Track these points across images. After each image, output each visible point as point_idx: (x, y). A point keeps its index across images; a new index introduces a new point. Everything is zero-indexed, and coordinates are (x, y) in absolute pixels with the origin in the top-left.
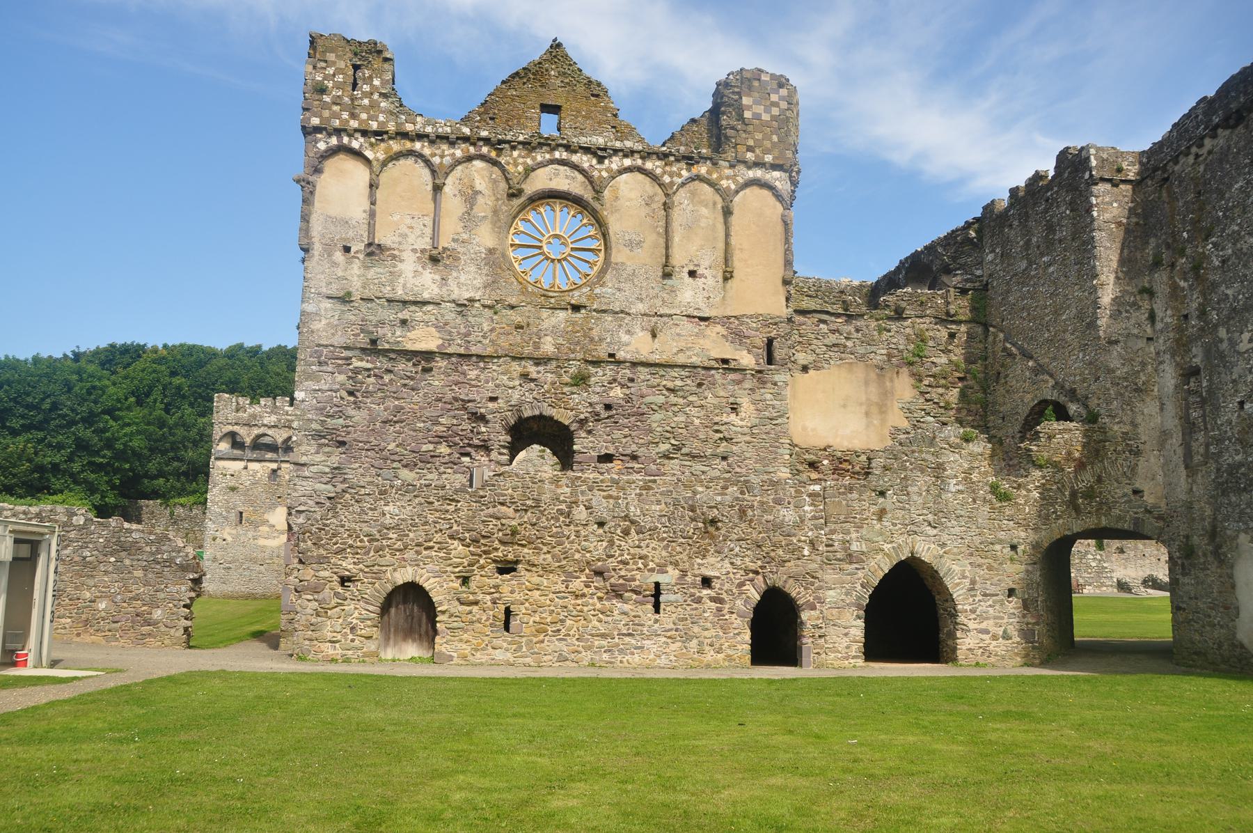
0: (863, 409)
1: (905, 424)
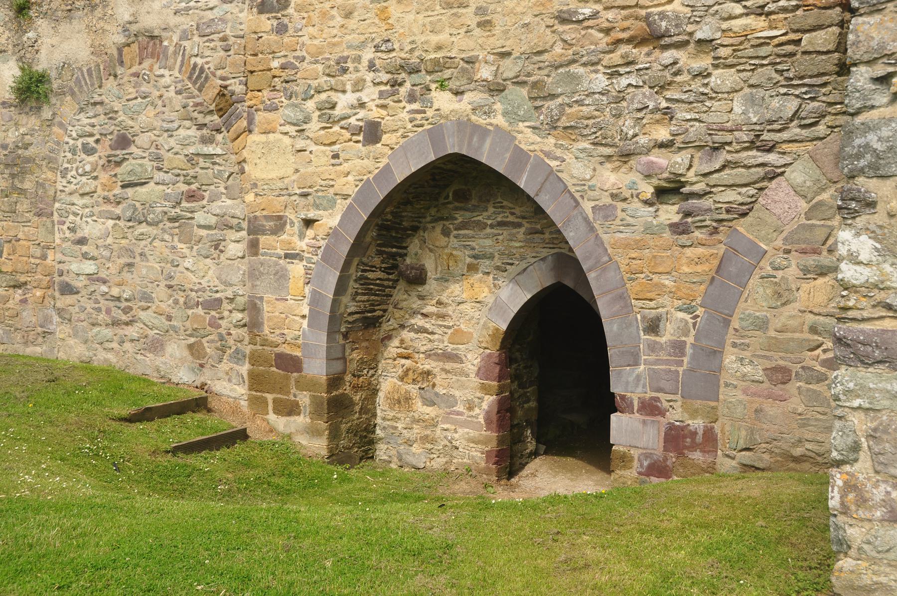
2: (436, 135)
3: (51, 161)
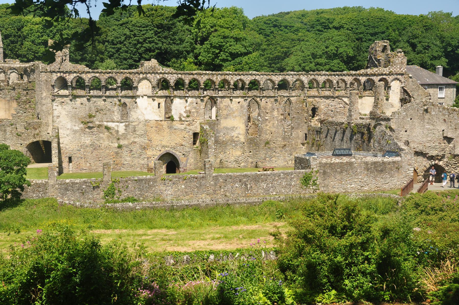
0: (4, 110)
1: (15, 113)
2: (166, 151)
3: (122, 153)
